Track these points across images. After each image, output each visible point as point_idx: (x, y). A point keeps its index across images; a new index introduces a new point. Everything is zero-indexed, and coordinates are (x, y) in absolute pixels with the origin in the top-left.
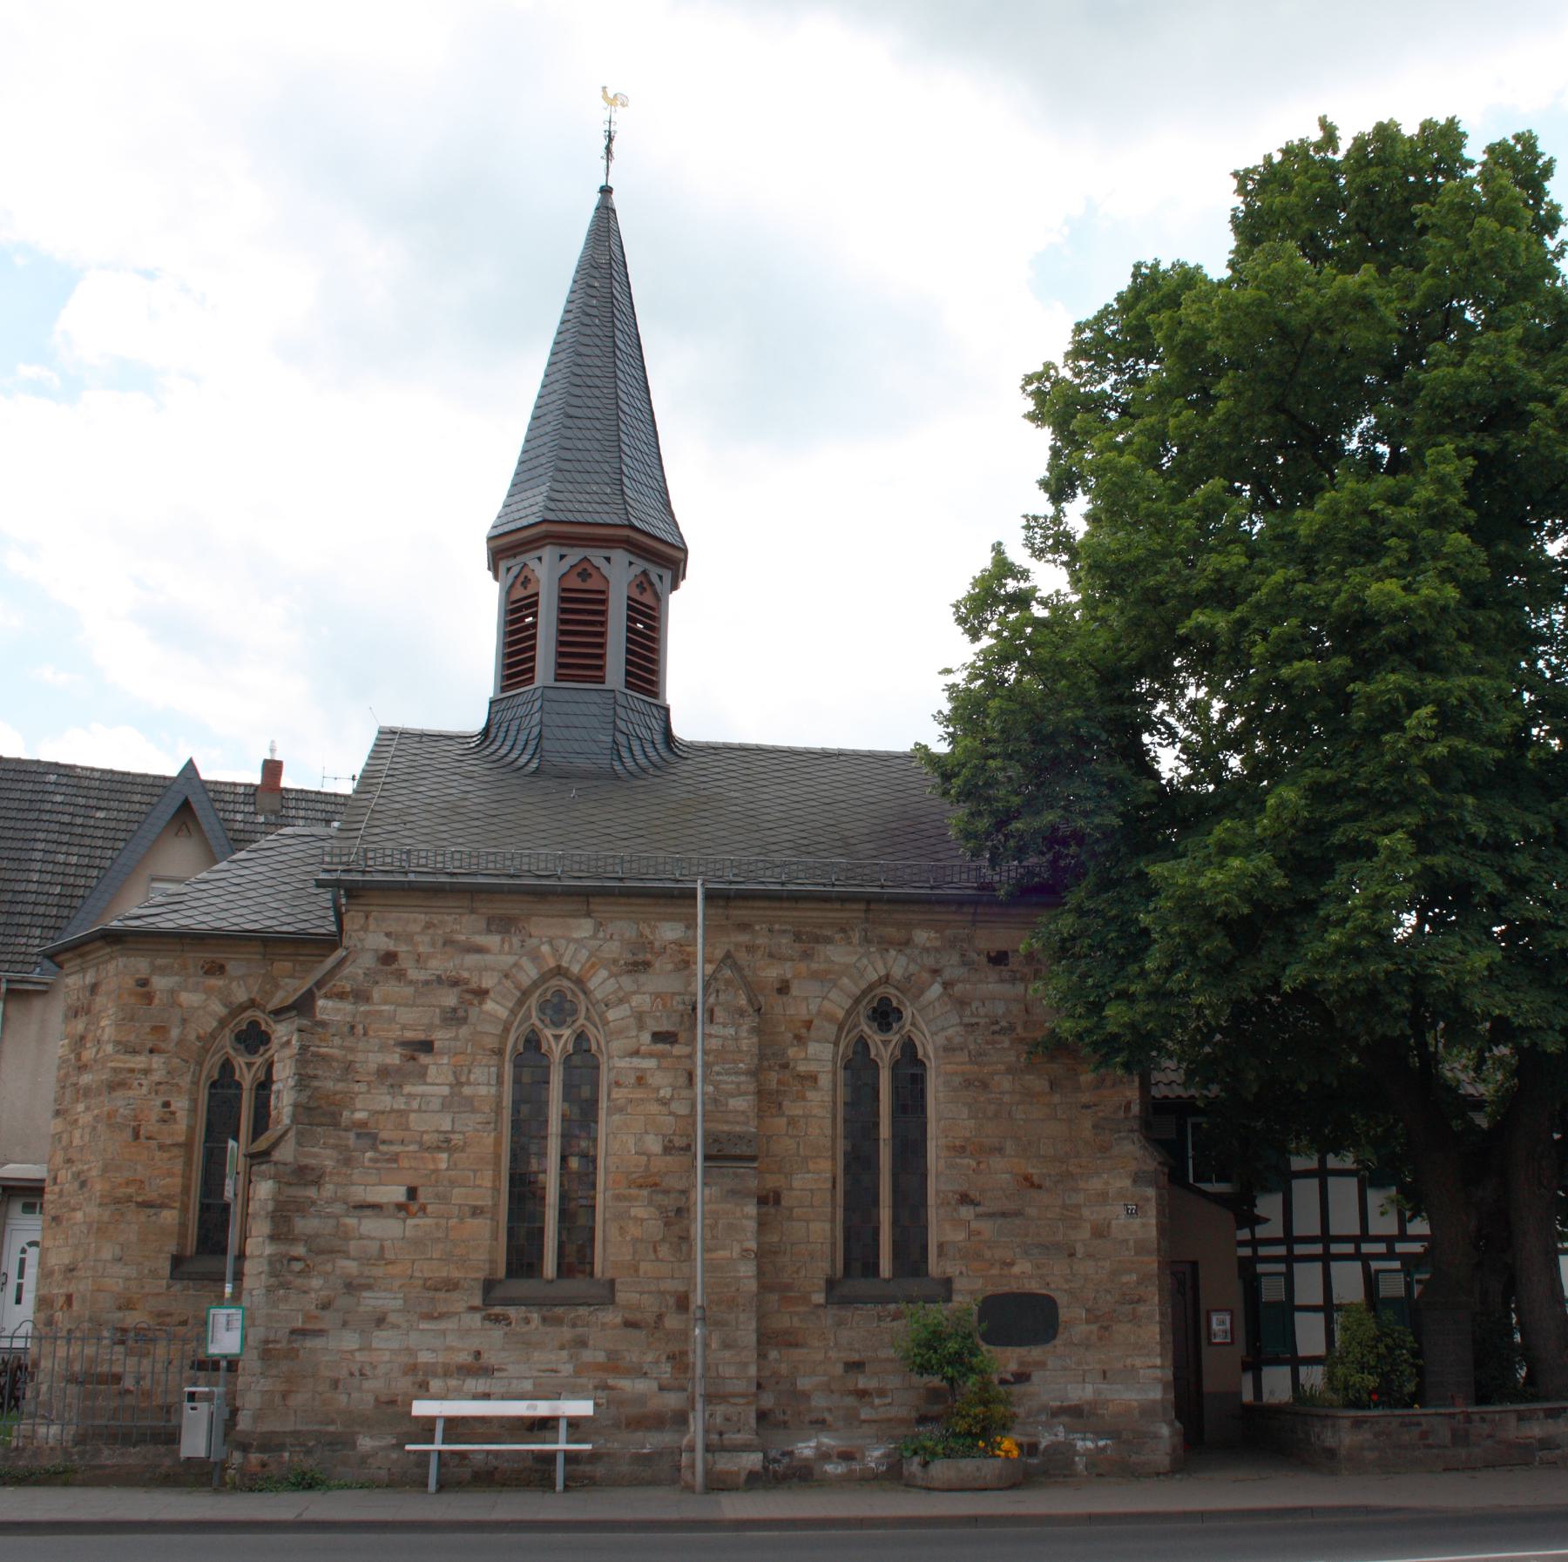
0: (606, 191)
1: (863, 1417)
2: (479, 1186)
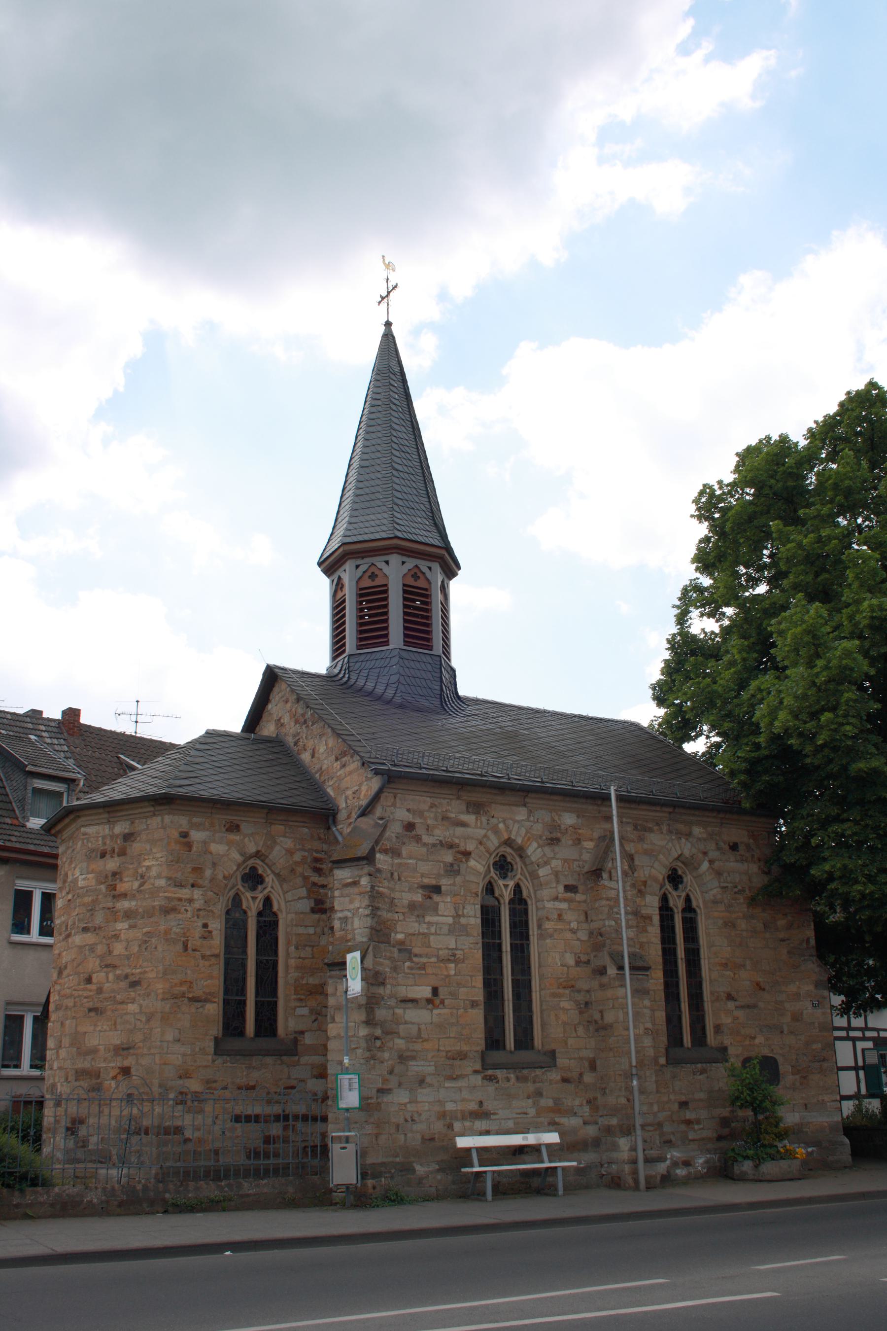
0: (388, 324)
1: (690, 1137)
2: (474, 987)
